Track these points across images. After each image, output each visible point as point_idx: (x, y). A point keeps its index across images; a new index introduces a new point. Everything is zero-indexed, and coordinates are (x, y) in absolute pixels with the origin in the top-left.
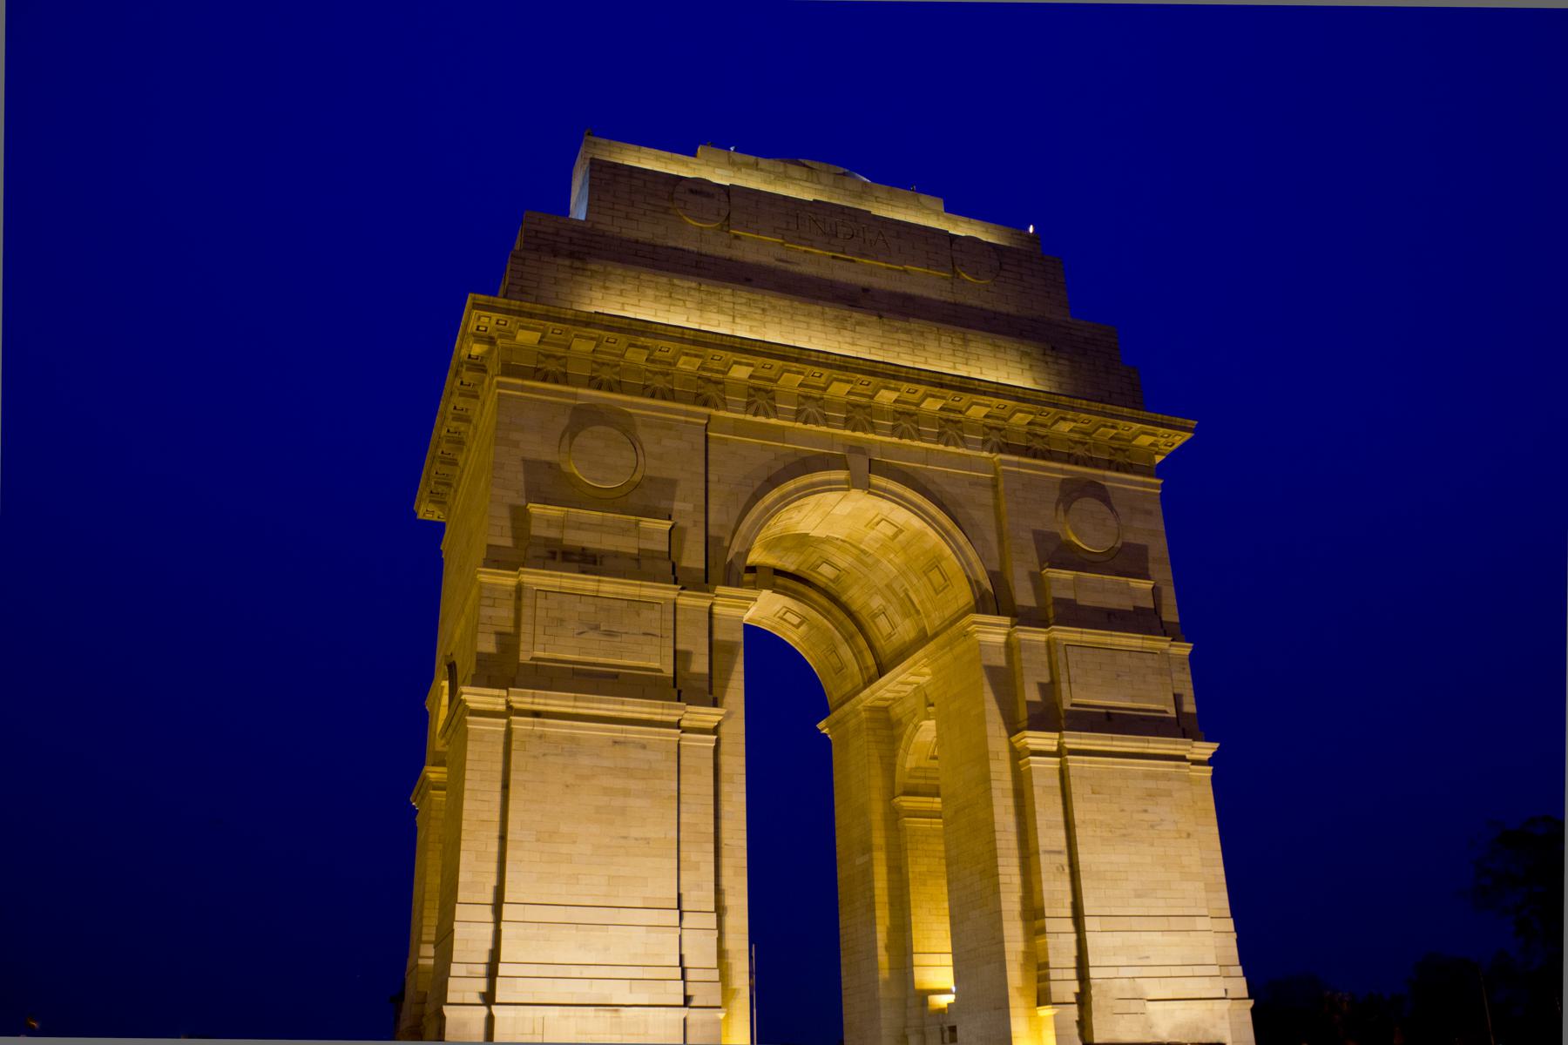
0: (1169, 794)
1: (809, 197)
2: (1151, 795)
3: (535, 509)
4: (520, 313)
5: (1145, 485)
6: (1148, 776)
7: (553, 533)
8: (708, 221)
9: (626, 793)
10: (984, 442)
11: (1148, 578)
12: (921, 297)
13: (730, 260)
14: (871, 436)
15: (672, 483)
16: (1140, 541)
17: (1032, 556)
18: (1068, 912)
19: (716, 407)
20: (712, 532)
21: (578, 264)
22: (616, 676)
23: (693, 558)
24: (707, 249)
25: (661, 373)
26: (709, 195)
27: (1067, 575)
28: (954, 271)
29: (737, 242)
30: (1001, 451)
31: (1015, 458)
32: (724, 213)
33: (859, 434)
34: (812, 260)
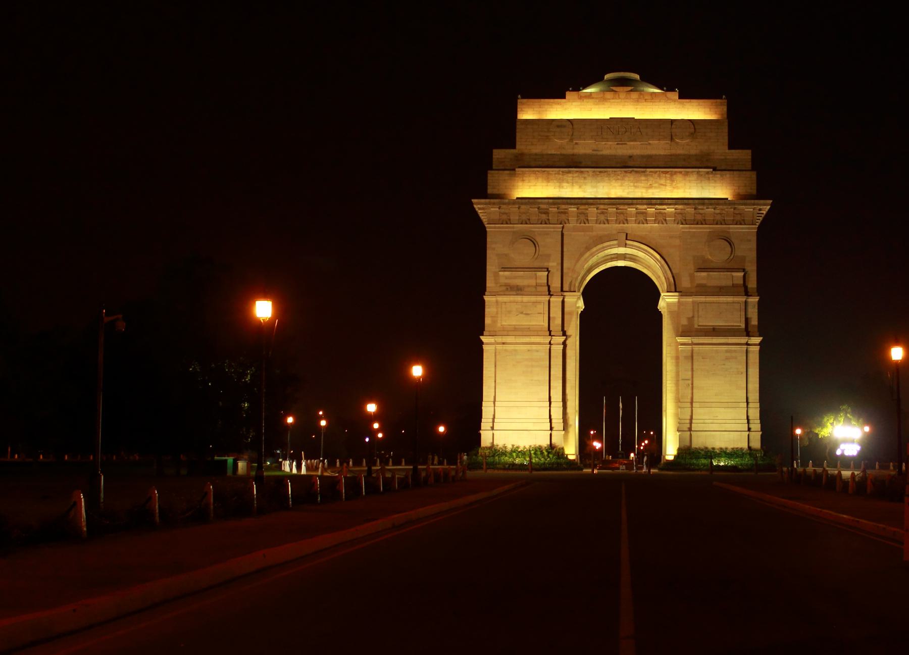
0: (736, 358)
1: (607, 117)
2: (727, 359)
3: (501, 273)
4: (490, 203)
5: (749, 228)
6: (727, 351)
7: (507, 281)
9: (532, 366)
11: (744, 270)
12: (656, 155)
13: (573, 155)
15: (549, 256)
18: (689, 400)
21: (512, 172)
23: (556, 284)
24: (564, 152)
26: (564, 126)
28: (672, 139)
32: (570, 133)
34: (609, 148)
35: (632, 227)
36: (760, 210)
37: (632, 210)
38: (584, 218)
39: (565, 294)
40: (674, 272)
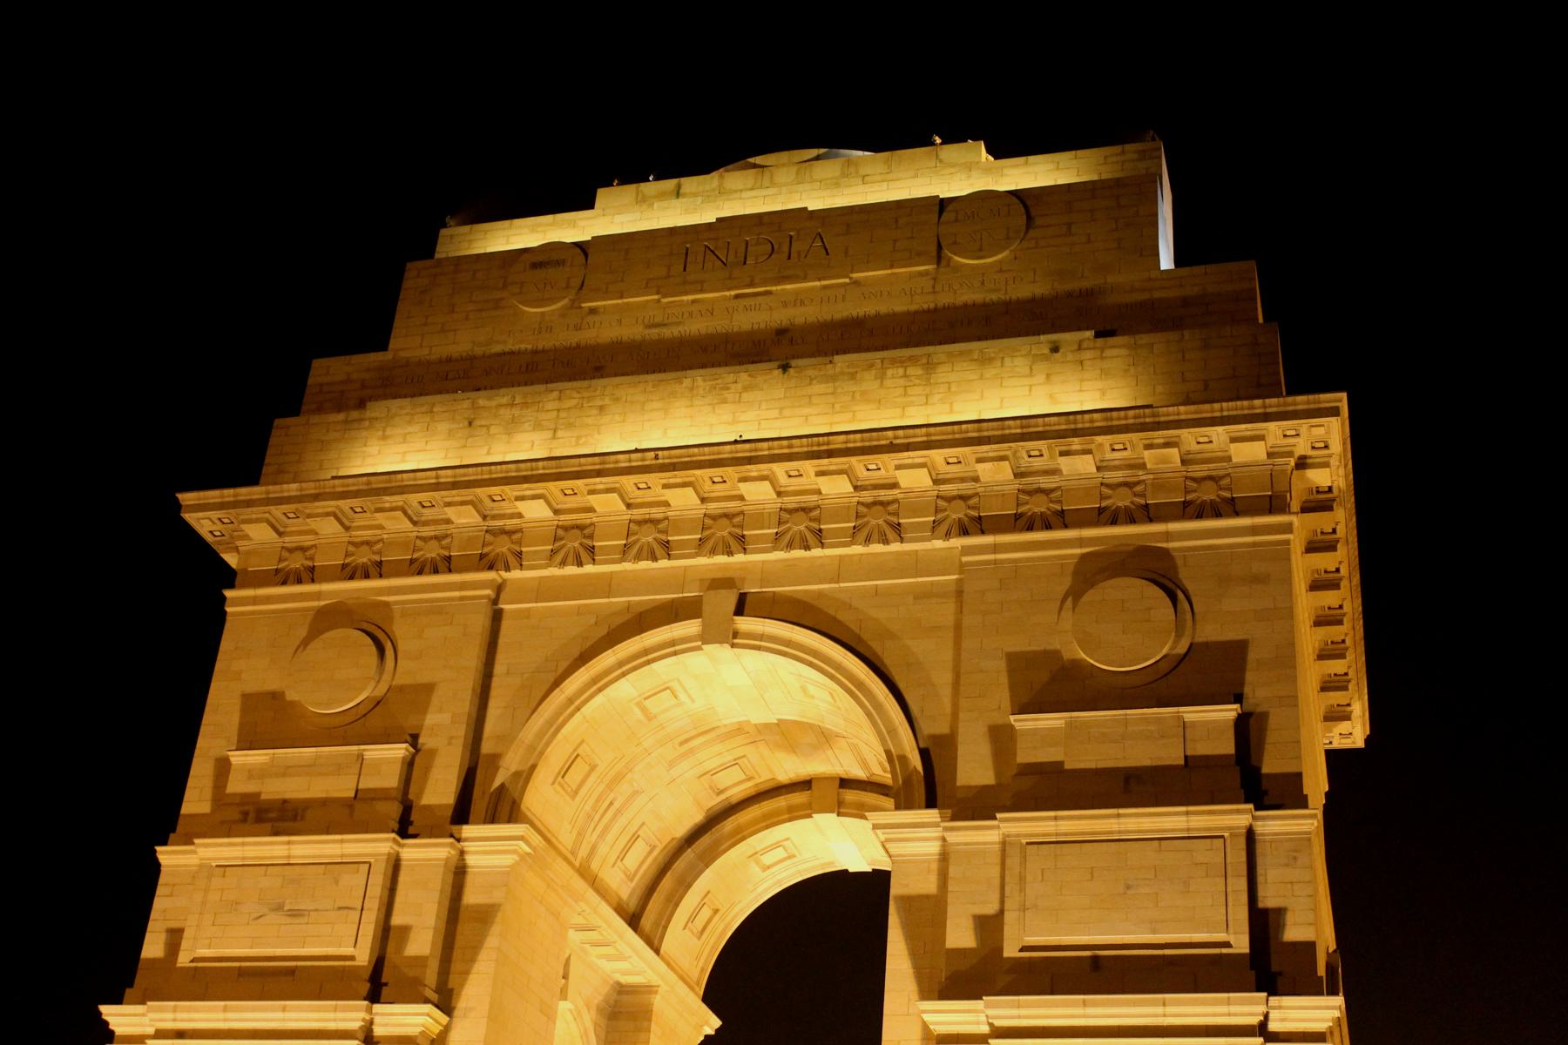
1: (710, 218)
5: (1254, 530)
7: (251, 787)
8: (551, 300)
10: (935, 525)
11: (1238, 699)
12: (878, 316)
14: (739, 558)
15: (429, 689)
16: (1231, 635)
17: (1003, 697)
19: (508, 569)
20: (487, 747)
21: (355, 414)
22: (291, 972)
25: (436, 538)
26: (559, 263)
27: (1052, 721)
28: (939, 258)
29: (590, 319)
30: (965, 532)
31: (988, 539)
32: (576, 283)
33: (721, 559)
35: (758, 563)
36: (1302, 463)
37: (758, 493)
38: (574, 539)
39: (468, 830)
40: (926, 728)
